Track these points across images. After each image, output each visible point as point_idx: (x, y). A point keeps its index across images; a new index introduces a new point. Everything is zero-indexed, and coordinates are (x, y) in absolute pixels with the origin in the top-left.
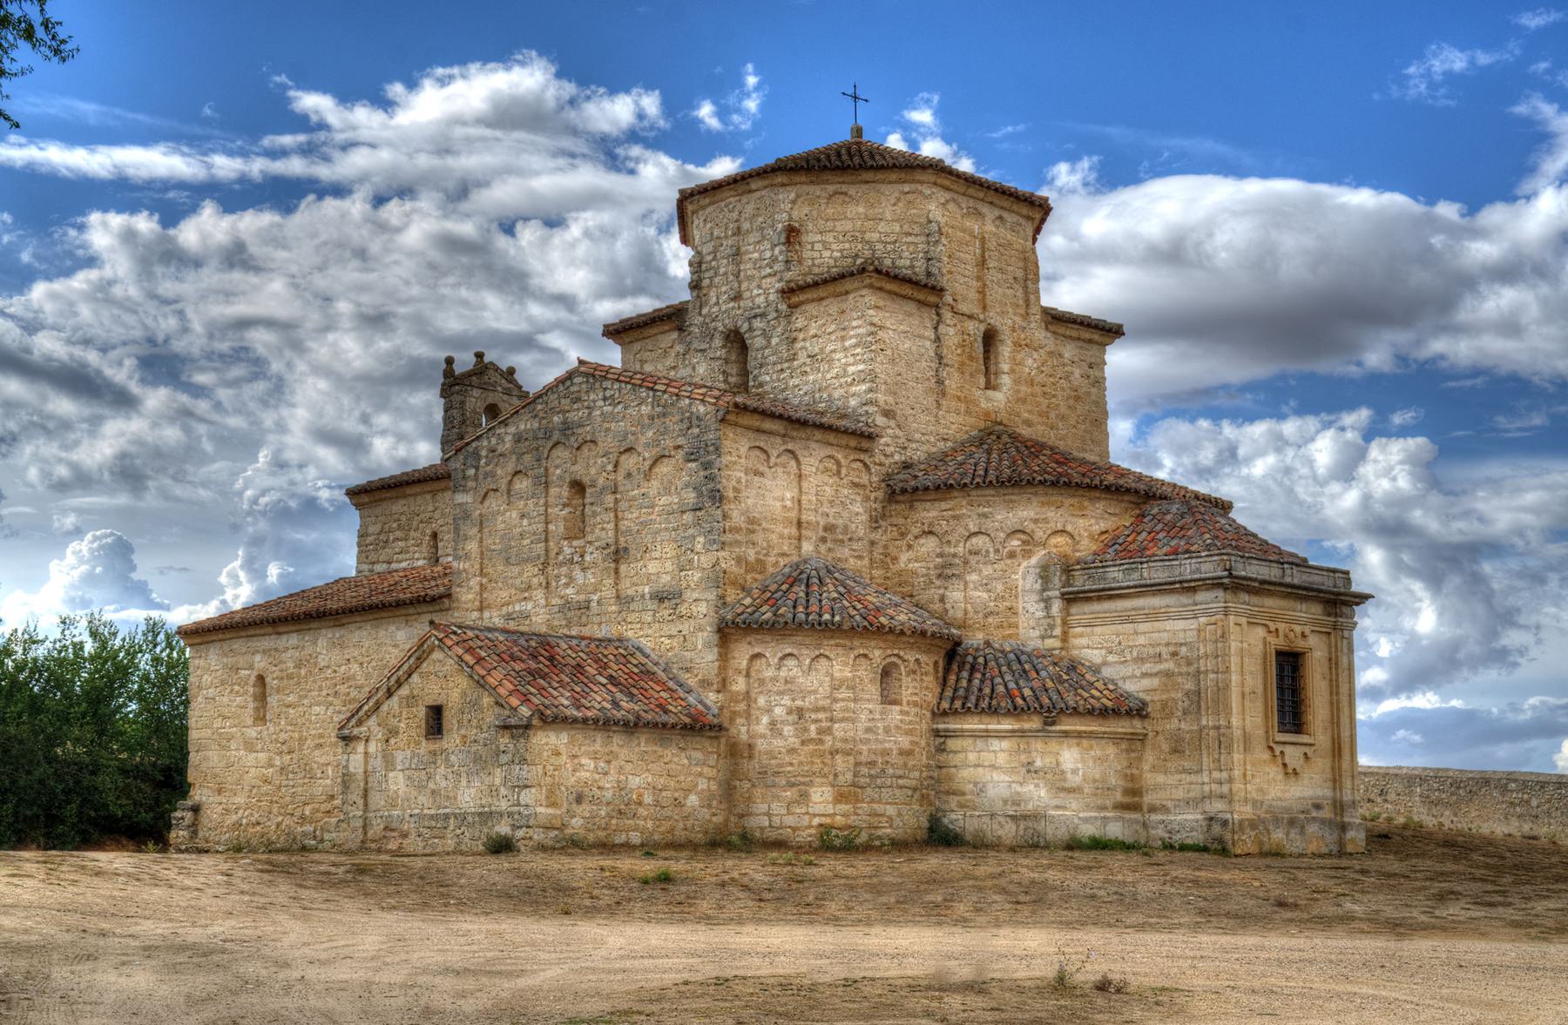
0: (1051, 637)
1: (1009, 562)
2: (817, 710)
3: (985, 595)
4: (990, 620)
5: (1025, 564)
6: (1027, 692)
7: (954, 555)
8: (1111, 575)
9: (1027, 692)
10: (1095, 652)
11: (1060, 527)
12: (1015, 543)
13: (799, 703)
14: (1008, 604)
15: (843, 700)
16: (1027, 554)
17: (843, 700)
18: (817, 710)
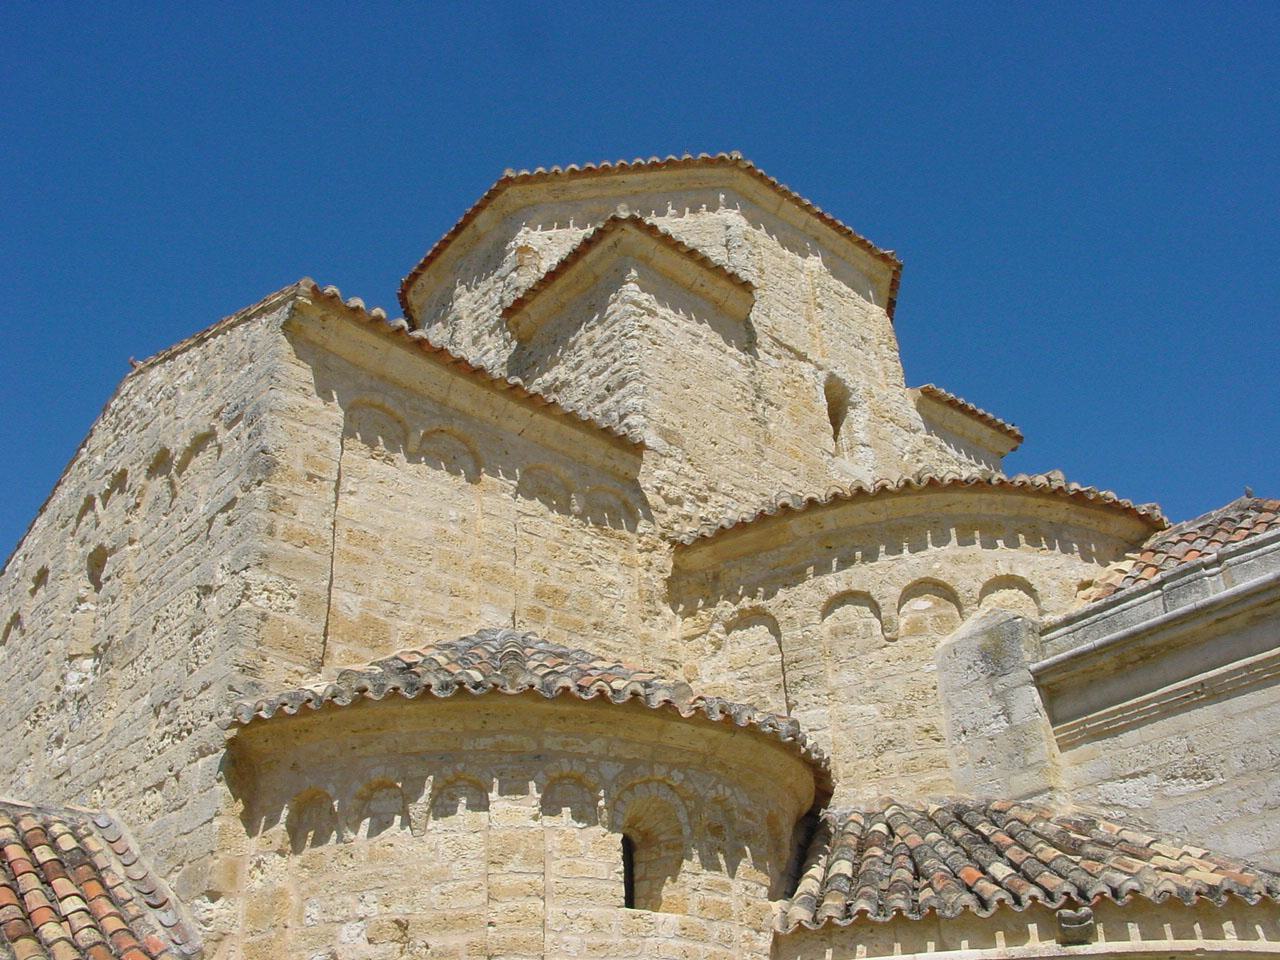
0: (1026, 767)
1: (913, 641)
2: (445, 924)
3: (873, 709)
4: (889, 756)
5: (945, 641)
6: (1000, 870)
7: (805, 641)
8: (1141, 611)
9: (1000, 870)
10: (1131, 784)
11: (1003, 571)
12: (921, 603)
13: (398, 910)
14: (923, 722)
15: (514, 892)
16: (944, 625)
17: (514, 892)
18: (445, 924)
